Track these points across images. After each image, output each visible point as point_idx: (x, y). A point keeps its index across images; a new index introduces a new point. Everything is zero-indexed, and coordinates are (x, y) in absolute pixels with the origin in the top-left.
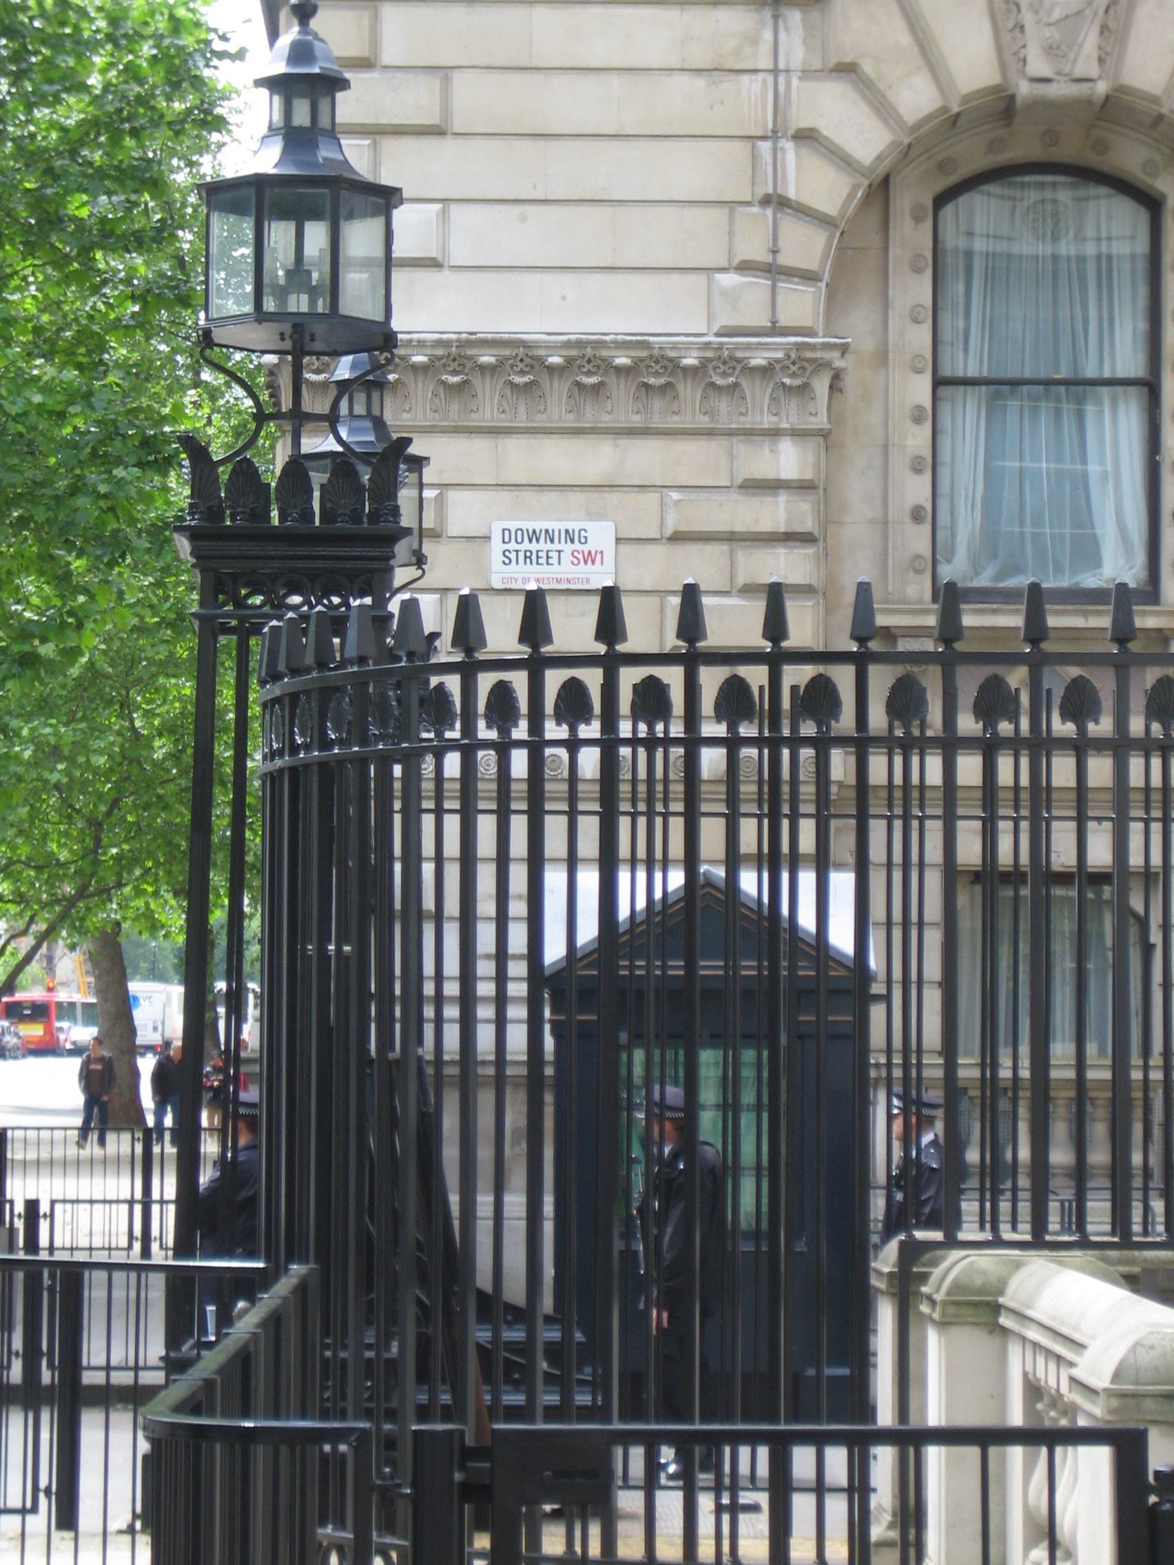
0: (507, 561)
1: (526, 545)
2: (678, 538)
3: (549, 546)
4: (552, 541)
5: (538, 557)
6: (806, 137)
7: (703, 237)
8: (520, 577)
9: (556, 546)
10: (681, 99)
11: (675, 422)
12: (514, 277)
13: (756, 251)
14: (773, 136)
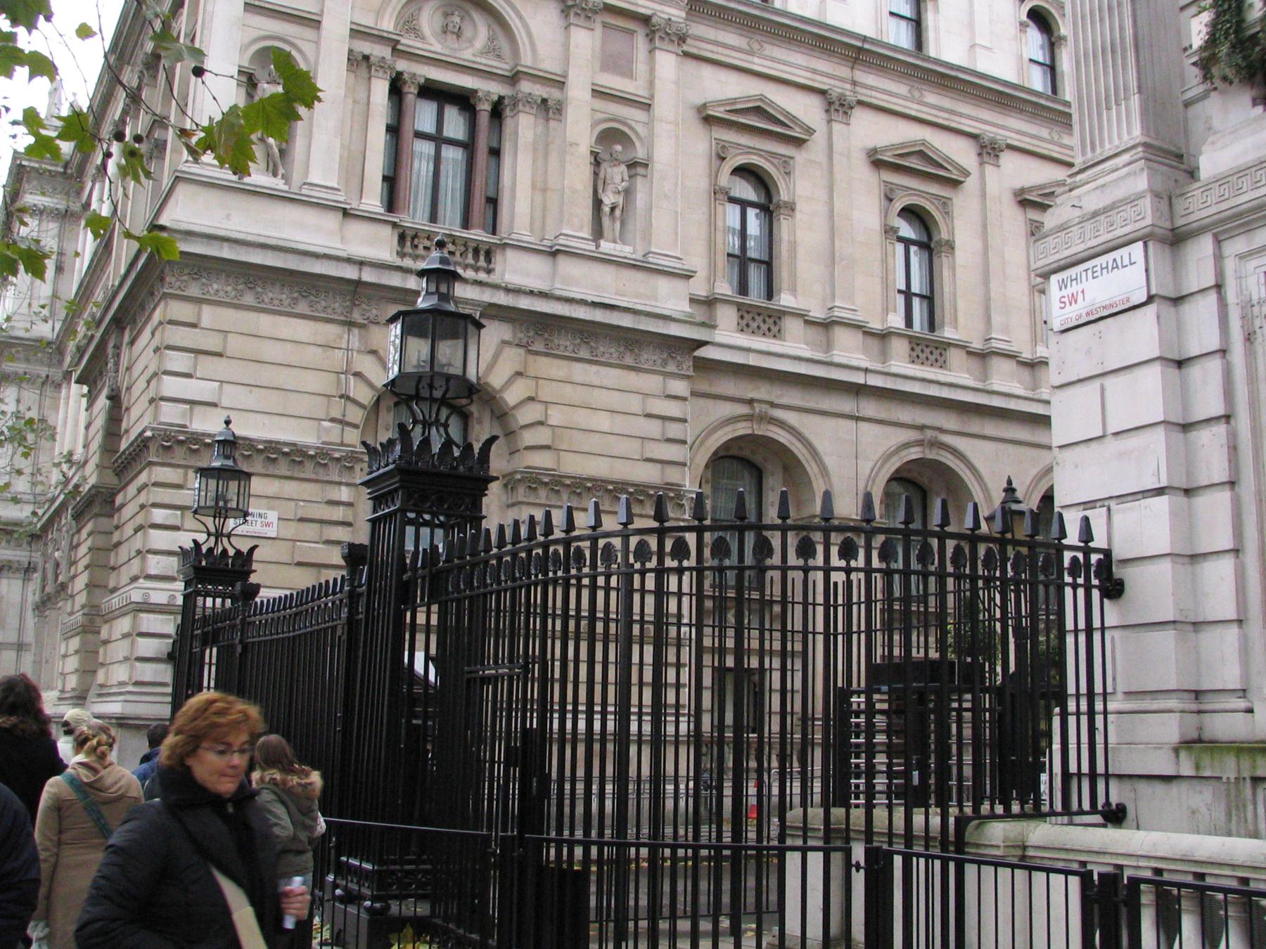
2: (301, 520)
6: (358, 375)
7: (317, 407)
10: (313, 355)
11: (302, 475)
12: (245, 414)
13: (336, 413)
14: (345, 373)
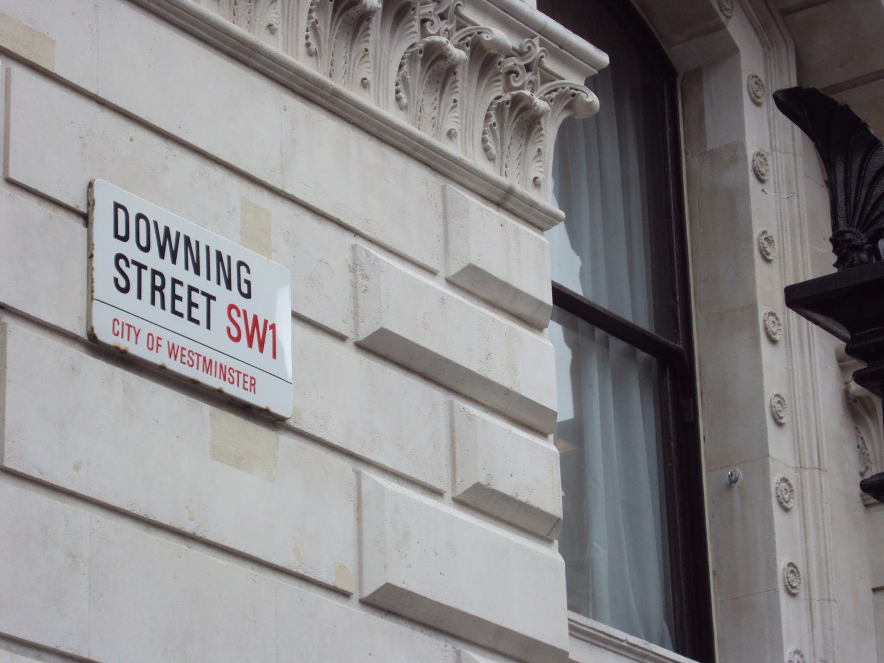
0: (122, 284)
1: (152, 259)
3: (189, 277)
4: (197, 272)
5: (175, 297)
8: (146, 328)
9: (199, 281)
